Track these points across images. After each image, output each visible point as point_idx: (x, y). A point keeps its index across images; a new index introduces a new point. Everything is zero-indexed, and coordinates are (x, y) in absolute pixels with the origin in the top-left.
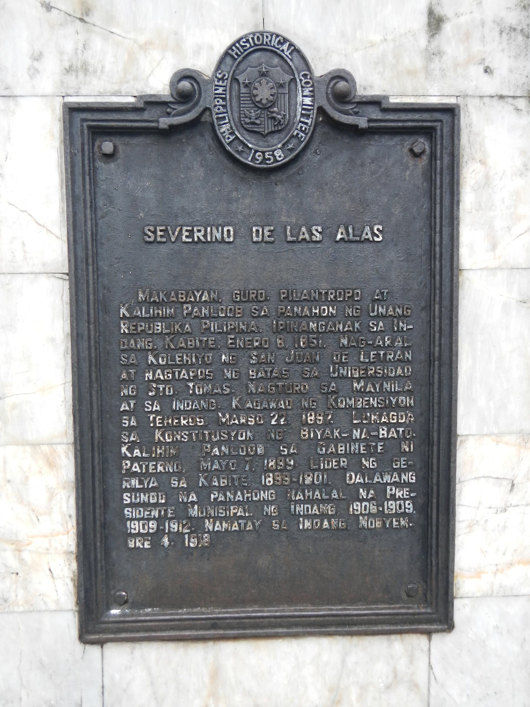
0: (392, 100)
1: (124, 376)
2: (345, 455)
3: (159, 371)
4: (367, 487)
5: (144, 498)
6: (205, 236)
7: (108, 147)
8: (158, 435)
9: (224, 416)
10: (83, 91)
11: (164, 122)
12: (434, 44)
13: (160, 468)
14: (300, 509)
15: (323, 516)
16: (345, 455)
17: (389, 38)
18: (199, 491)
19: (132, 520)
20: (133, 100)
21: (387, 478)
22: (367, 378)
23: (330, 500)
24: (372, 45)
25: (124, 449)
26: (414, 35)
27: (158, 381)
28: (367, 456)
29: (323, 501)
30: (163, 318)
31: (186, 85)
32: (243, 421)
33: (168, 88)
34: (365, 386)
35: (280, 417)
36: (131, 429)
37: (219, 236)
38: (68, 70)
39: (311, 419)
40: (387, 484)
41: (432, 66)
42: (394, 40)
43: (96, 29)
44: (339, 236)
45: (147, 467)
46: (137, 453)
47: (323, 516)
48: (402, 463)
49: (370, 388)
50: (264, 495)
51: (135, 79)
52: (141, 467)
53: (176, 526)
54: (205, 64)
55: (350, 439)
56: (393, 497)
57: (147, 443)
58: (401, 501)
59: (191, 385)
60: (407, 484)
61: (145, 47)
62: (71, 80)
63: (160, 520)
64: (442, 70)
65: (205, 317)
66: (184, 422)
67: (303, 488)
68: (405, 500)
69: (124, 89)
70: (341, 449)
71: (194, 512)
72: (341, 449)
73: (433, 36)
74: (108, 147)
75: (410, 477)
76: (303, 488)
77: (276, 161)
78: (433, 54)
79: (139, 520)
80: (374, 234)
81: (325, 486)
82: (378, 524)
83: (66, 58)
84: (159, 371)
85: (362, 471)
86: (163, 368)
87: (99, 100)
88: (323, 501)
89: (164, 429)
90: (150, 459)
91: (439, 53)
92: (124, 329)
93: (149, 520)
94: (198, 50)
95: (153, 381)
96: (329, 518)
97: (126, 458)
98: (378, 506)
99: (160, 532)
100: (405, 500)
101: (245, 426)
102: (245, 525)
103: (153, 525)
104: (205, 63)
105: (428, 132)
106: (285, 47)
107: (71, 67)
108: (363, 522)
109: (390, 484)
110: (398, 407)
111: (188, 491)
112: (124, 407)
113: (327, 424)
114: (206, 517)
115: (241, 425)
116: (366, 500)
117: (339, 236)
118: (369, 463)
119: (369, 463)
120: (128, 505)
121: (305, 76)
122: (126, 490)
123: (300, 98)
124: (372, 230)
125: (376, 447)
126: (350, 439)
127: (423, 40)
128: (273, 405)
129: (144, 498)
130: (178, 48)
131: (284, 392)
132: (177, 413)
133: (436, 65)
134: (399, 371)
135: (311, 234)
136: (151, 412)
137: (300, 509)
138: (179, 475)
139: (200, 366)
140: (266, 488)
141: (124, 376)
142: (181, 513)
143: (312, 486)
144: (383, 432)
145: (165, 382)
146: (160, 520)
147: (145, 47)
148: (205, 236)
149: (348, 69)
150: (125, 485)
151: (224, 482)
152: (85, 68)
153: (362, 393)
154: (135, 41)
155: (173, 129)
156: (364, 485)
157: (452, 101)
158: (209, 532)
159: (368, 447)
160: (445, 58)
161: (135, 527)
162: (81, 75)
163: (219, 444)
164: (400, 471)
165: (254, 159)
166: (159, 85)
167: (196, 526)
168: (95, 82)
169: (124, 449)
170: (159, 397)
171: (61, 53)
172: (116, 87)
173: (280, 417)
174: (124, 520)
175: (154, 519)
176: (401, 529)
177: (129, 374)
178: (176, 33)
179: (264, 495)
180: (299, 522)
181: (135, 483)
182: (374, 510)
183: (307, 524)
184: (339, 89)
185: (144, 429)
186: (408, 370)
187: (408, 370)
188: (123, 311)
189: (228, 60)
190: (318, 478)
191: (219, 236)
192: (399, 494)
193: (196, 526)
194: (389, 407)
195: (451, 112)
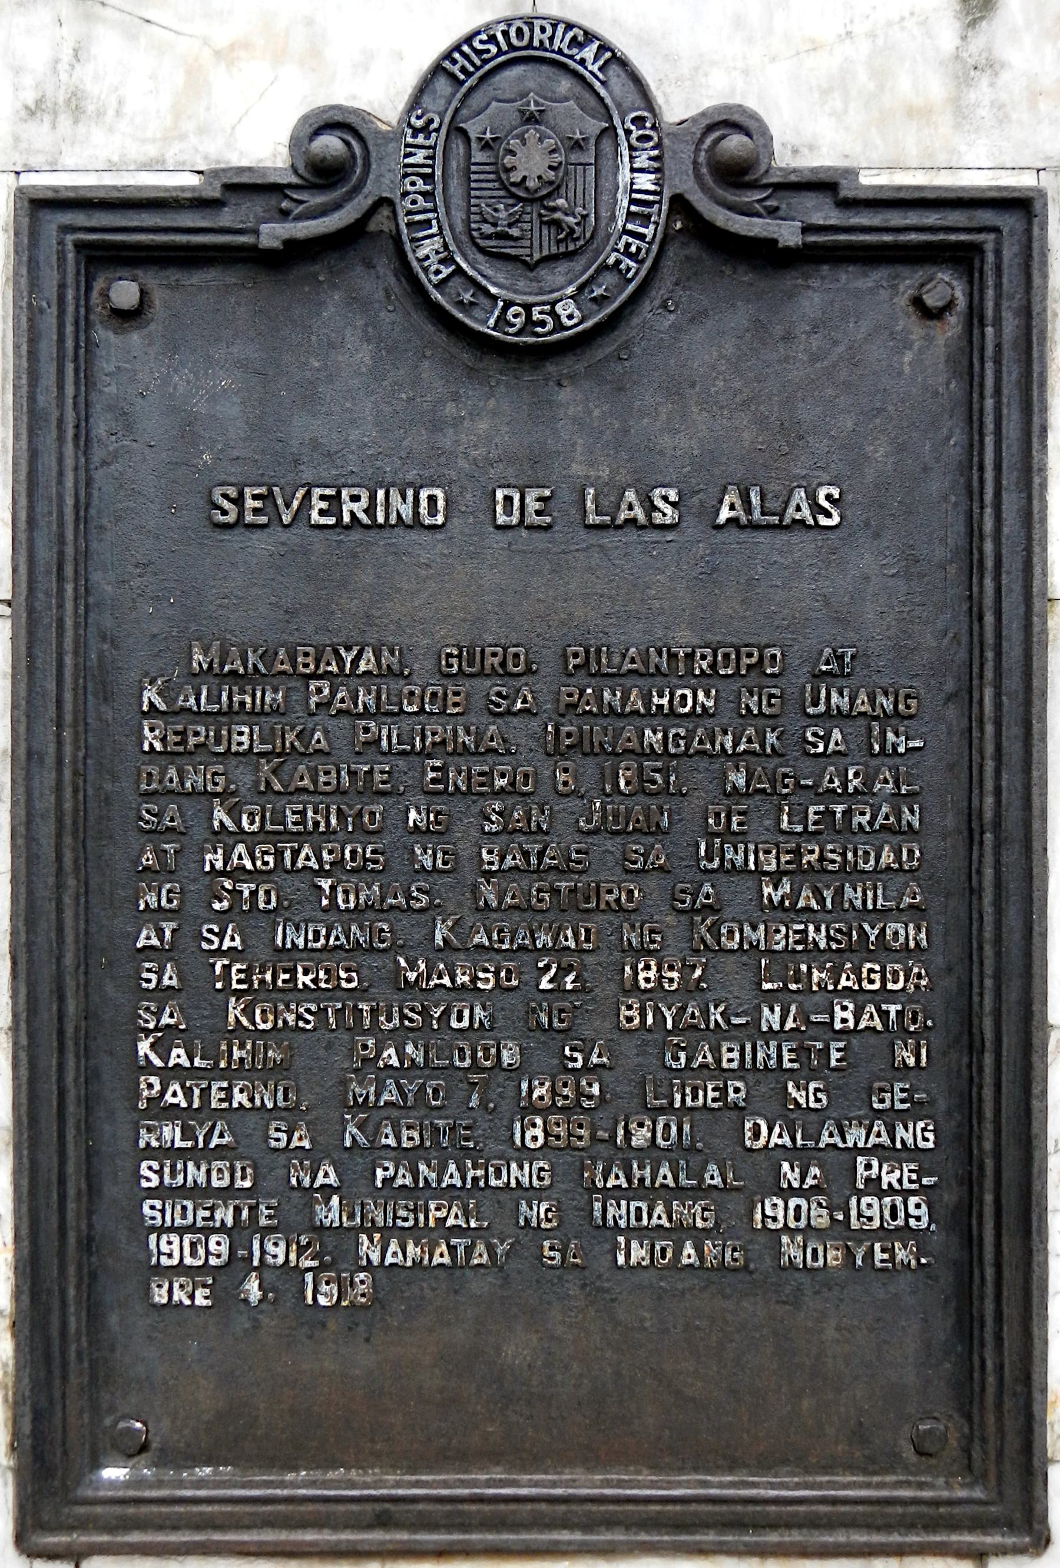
0: (866, 179)
1: (148, 859)
2: (741, 1072)
3: (241, 848)
4: (801, 1156)
5: (195, 1174)
6: (370, 511)
7: (125, 292)
8: (235, 1011)
9: (413, 966)
10: (69, 160)
11: (273, 234)
12: (978, 42)
13: (239, 1098)
14: (618, 1212)
15: (680, 1231)
16: (741, 1072)
17: (860, 28)
18: (343, 1157)
19: (161, 1230)
20: (194, 180)
21: (856, 1136)
22: (798, 872)
23: (700, 1191)
24: (815, 47)
25: (144, 1047)
26: (924, 23)
27: (238, 874)
28: (803, 1076)
29: (679, 1192)
30: (255, 715)
31: (331, 144)
32: (463, 979)
33: (285, 151)
34: (795, 894)
35: (564, 971)
36: (163, 993)
37: (406, 511)
38: (33, 111)
39: (647, 977)
40: (857, 1150)
41: (972, 96)
42: (872, 35)
43: (108, 12)
44: (725, 514)
45: (206, 1092)
46: (178, 1056)
47: (680, 1231)
48: (897, 1097)
49: (806, 899)
50: (517, 1173)
51: (202, 130)
52: (188, 1093)
53: (280, 1251)
54: (383, 93)
55: (754, 1031)
56: (874, 1186)
57: (206, 1032)
58: (895, 1198)
59: (326, 884)
60: (911, 1152)
61: (227, 55)
62: (40, 135)
63: (236, 1233)
64: (998, 106)
65: (366, 714)
66: (303, 979)
67: (626, 1156)
68: (906, 1194)
69: (173, 154)
70: (730, 1058)
71: (331, 1213)
72: (730, 1058)
73: (973, 24)
74: (125, 292)
75: (917, 1134)
76: (626, 1156)
77: (559, 327)
78: (971, 69)
79: (181, 1231)
80: (817, 509)
81: (683, 1152)
82: (834, 1257)
83: (28, 81)
84: (241, 848)
85: (789, 1115)
86: (251, 840)
87: (109, 180)
88: (679, 1192)
89: (251, 997)
90: (212, 1073)
91: (990, 66)
92: (151, 739)
93: (208, 1231)
94: (364, 65)
95: (223, 873)
96: (699, 1237)
97: (149, 1068)
98: (831, 1208)
99: (239, 1263)
100: (906, 1194)
101: (472, 989)
102: (469, 1250)
103: (219, 1246)
104: (383, 93)
105: (964, 258)
106: (589, 53)
107: (39, 102)
108: (791, 1250)
109: (863, 1152)
110: (883, 949)
111: (313, 1159)
112: (146, 938)
113: (690, 990)
114: (362, 1229)
115: (458, 989)
116: (799, 1192)
117: (725, 514)
118: (805, 1096)
119: (805, 1096)
120: (151, 1193)
121: (639, 121)
122: (149, 1152)
123: (624, 176)
124: (812, 498)
125: (826, 1052)
126: (754, 1031)
127: (947, 33)
128: (544, 939)
129: (195, 1174)
130: (314, 55)
131: (577, 905)
132: (287, 957)
133: (982, 92)
134: (887, 857)
135: (651, 508)
136: (219, 952)
137: (618, 1212)
138: (291, 1116)
139: (350, 838)
140: (524, 1154)
141: (148, 859)
142: (296, 1218)
143: (652, 1152)
144: (843, 1015)
145: (255, 875)
146: (236, 1233)
147: (227, 55)
148: (370, 511)
149: (751, 103)
150: (145, 1138)
151: (410, 1138)
152: (76, 105)
153: (787, 910)
154: (206, 42)
155: (297, 252)
156: (792, 1153)
157: (1027, 180)
158: (369, 1267)
159: (802, 1052)
160: (1005, 76)
161: (171, 1249)
162: (65, 121)
163: (398, 1037)
164: (892, 1118)
165: (502, 321)
166: (263, 144)
167: (334, 1251)
168: (98, 135)
169: (144, 1047)
170: (240, 913)
171: (18, 71)
172: (152, 151)
173: (564, 971)
174: (142, 1230)
175: (223, 1229)
176: (893, 1270)
177: (160, 853)
178: (310, 22)
179: (517, 1173)
180: (616, 1246)
181: (171, 1133)
182: (821, 1218)
183: (638, 1253)
184: (730, 152)
185: (199, 994)
186: (912, 853)
187: (912, 853)
188: (150, 695)
189: (442, 85)
190: (666, 1131)
191: (406, 511)
192: (889, 1179)
193: (334, 1251)
194: (859, 950)
195: (1023, 206)
